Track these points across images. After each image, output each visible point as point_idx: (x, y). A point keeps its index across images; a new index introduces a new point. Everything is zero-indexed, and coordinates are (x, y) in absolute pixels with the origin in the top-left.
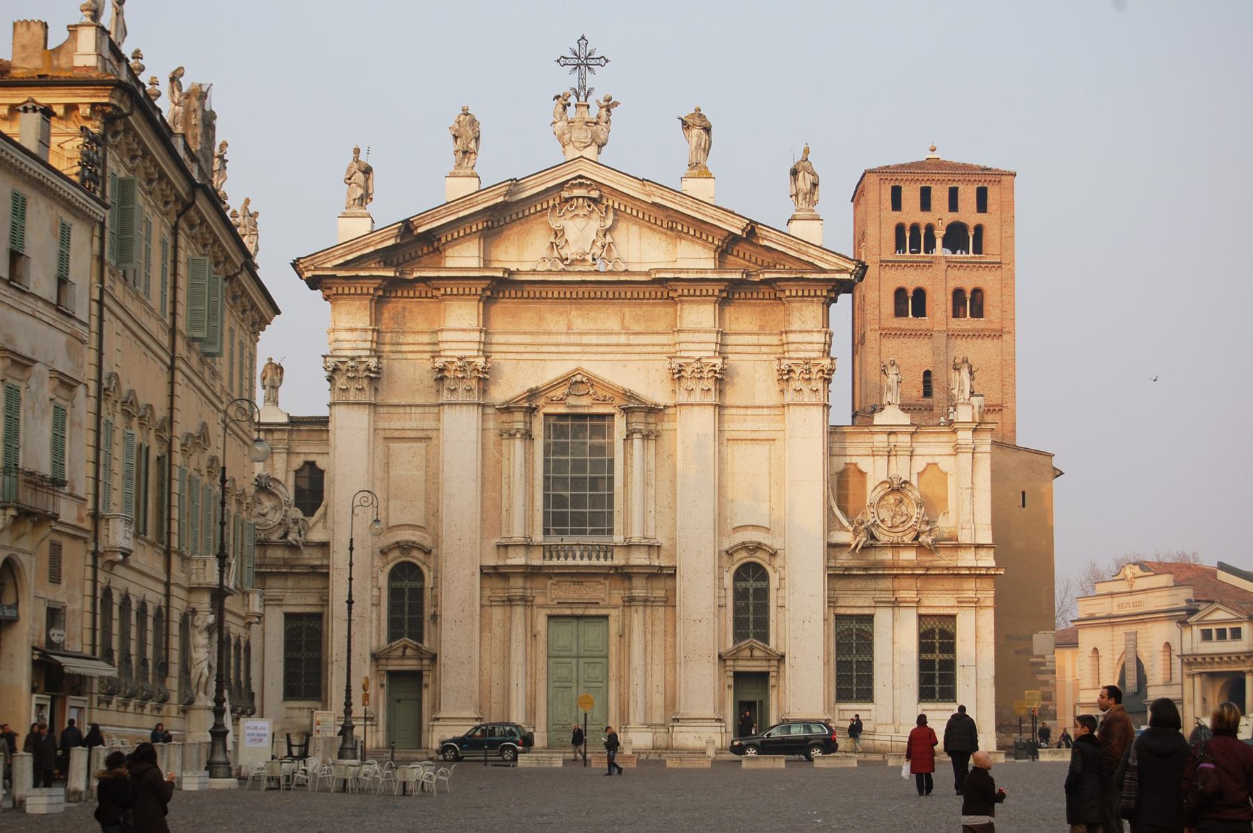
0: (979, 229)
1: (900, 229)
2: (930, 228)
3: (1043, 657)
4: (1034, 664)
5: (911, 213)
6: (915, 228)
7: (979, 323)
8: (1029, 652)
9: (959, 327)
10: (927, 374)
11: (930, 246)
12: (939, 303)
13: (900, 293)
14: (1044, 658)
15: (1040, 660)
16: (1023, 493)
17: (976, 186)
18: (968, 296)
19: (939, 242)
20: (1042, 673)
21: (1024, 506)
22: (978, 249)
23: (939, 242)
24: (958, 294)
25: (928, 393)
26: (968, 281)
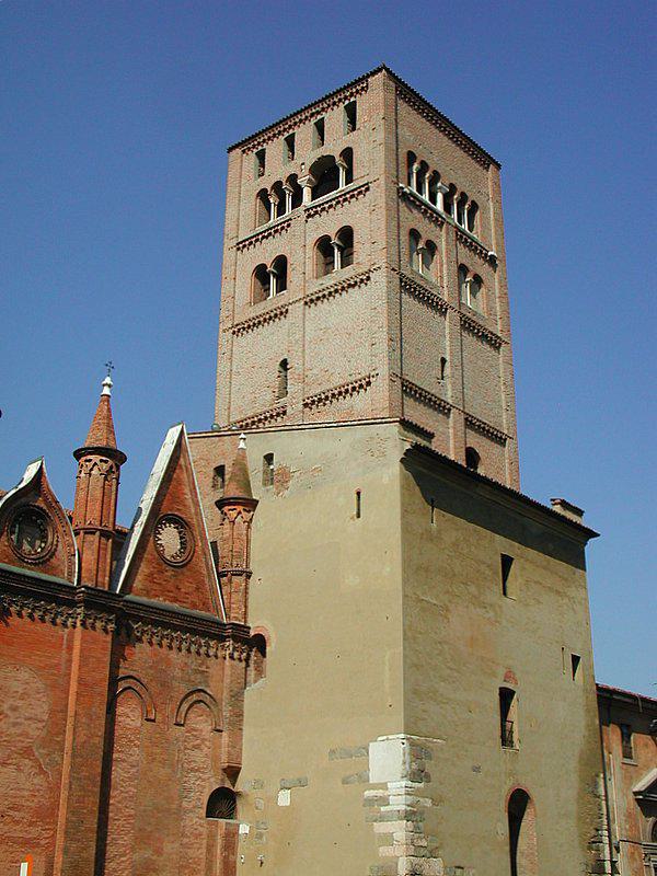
0: (348, 154)
1: (263, 195)
2: (293, 178)
3: (384, 786)
4: (370, 802)
5: (278, 170)
6: (277, 186)
7: (349, 272)
8: (363, 779)
9: (323, 287)
10: (284, 364)
11: (297, 201)
12: (303, 262)
13: (261, 274)
14: (384, 786)
15: (380, 793)
16: (358, 494)
17: (342, 106)
18: (335, 240)
19: (307, 193)
20: (382, 818)
21: (359, 516)
22: (349, 180)
23: (307, 193)
24: (324, 246)
25: (284, 392)
26: (329, 225)
